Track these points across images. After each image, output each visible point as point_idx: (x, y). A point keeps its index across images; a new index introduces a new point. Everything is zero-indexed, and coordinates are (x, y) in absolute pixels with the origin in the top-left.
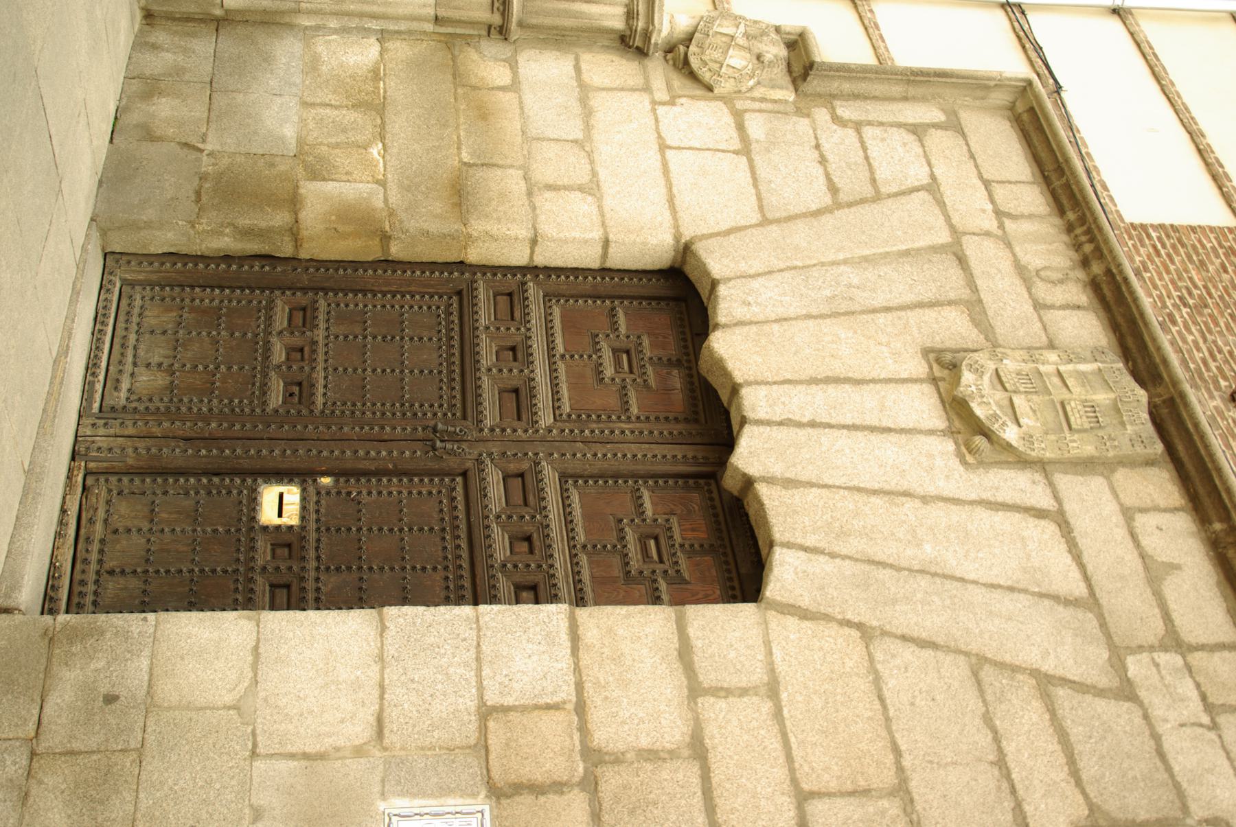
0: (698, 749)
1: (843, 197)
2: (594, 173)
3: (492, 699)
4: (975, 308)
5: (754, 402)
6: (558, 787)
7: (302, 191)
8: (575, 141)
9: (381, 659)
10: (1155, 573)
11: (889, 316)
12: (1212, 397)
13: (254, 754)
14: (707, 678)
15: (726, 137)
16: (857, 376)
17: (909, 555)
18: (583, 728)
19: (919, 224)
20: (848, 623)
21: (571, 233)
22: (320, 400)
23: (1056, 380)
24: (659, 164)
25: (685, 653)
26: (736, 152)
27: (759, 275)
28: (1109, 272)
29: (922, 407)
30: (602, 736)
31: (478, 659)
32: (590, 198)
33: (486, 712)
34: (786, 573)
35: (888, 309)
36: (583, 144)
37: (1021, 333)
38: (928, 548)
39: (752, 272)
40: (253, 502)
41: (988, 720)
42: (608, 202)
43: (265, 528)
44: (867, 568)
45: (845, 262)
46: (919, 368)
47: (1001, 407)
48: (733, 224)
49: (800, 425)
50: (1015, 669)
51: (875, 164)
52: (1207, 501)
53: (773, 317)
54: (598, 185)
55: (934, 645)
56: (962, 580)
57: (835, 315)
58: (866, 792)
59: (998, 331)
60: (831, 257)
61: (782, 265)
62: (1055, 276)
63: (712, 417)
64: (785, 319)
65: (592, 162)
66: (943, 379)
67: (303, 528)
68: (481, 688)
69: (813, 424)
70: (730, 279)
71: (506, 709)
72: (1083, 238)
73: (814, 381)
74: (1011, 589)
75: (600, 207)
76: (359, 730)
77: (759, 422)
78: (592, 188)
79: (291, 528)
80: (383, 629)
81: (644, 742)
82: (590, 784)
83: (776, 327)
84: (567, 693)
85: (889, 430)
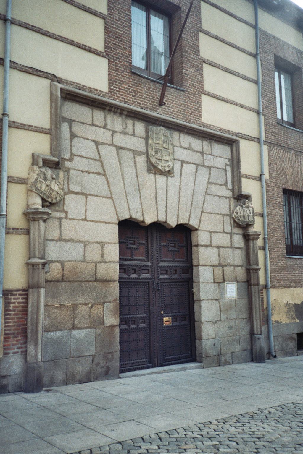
0: (218, 247)
1: (102, 172)
2: (97, 243)
3: (213, 281)
4: (135, 153)
5: (162, 218)
6: (223, 272)
7: (108, 325)
8: (85, 246)
9: (208, 300)
10: (190, 148)
11: (139, 177)
12: (159, 109)
13: (220, 320)
14: (209, 244)
15: (81, 199)
16: (155, 192)
17: (190, 197)
18: (216, 266)
19: (109, 154)
20: (201, 214)
21: (113, 252)
22: (144, 315)
23: (157, 145)
24: (93, 223)
25: (206, 246)
26: (86, 198)
27: (128, 206)
28: (128, 112)
29: (161, 180)
30: (217, 263)
31: (207, 283)
32: (106, 246)
33: (214, 282)
34: (194, 223)
35: (137, 176)
36: (85, 244)
37: (141, 144)
38: (189, 193)
39: (128, 207)
40: (167, 327)
41: (214, 196)
42: (107, 241)
43: (172, 324)
44: (192, 207)
45: (123, 181)
46: (152, 176)
47: (165, 163)
48: (113, 207)
49: (166, 210)
50: (207, 187)
51: (88, 156)
52: (181, 129)
53: (140, 206)
54: (101, 242)
55: (204, 200)
56: (194, 189)
57: (139, 190)
58: (223, 221)
59: (141, 150)
60: (122, 184)
61: (125, 198)
62: (124, 125)
63: (159, 227)
64: (141, 204)
65: (93, 243)
66: (155, 172)
67: (172, 316)
68: (211, 283)
69: (166, 207)
70: (130, 214)
71: (214, 279)
72: (116, 110)
73: (156, 202)
74: (195, 180)
75: (109, 243)
76: (217, 303)
77: (166, 219)
78: (102, 245)
79: (172, 319)
80: (204, 300)
81: (217, 256)
82: (223, 266)
83: (143, 207)
84: (212, 268)
85: (167, 190)
